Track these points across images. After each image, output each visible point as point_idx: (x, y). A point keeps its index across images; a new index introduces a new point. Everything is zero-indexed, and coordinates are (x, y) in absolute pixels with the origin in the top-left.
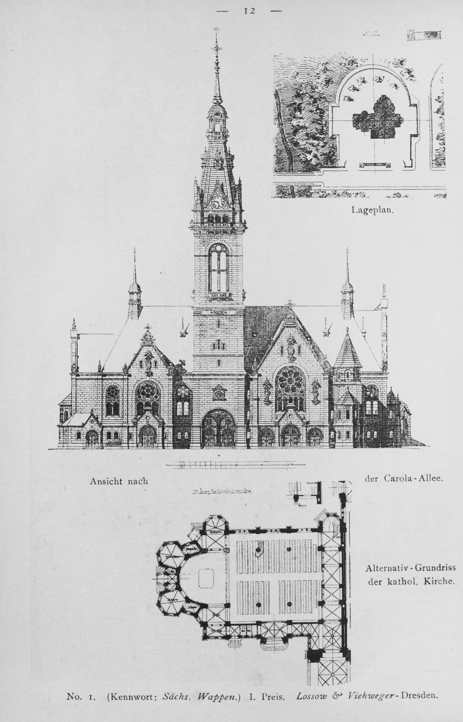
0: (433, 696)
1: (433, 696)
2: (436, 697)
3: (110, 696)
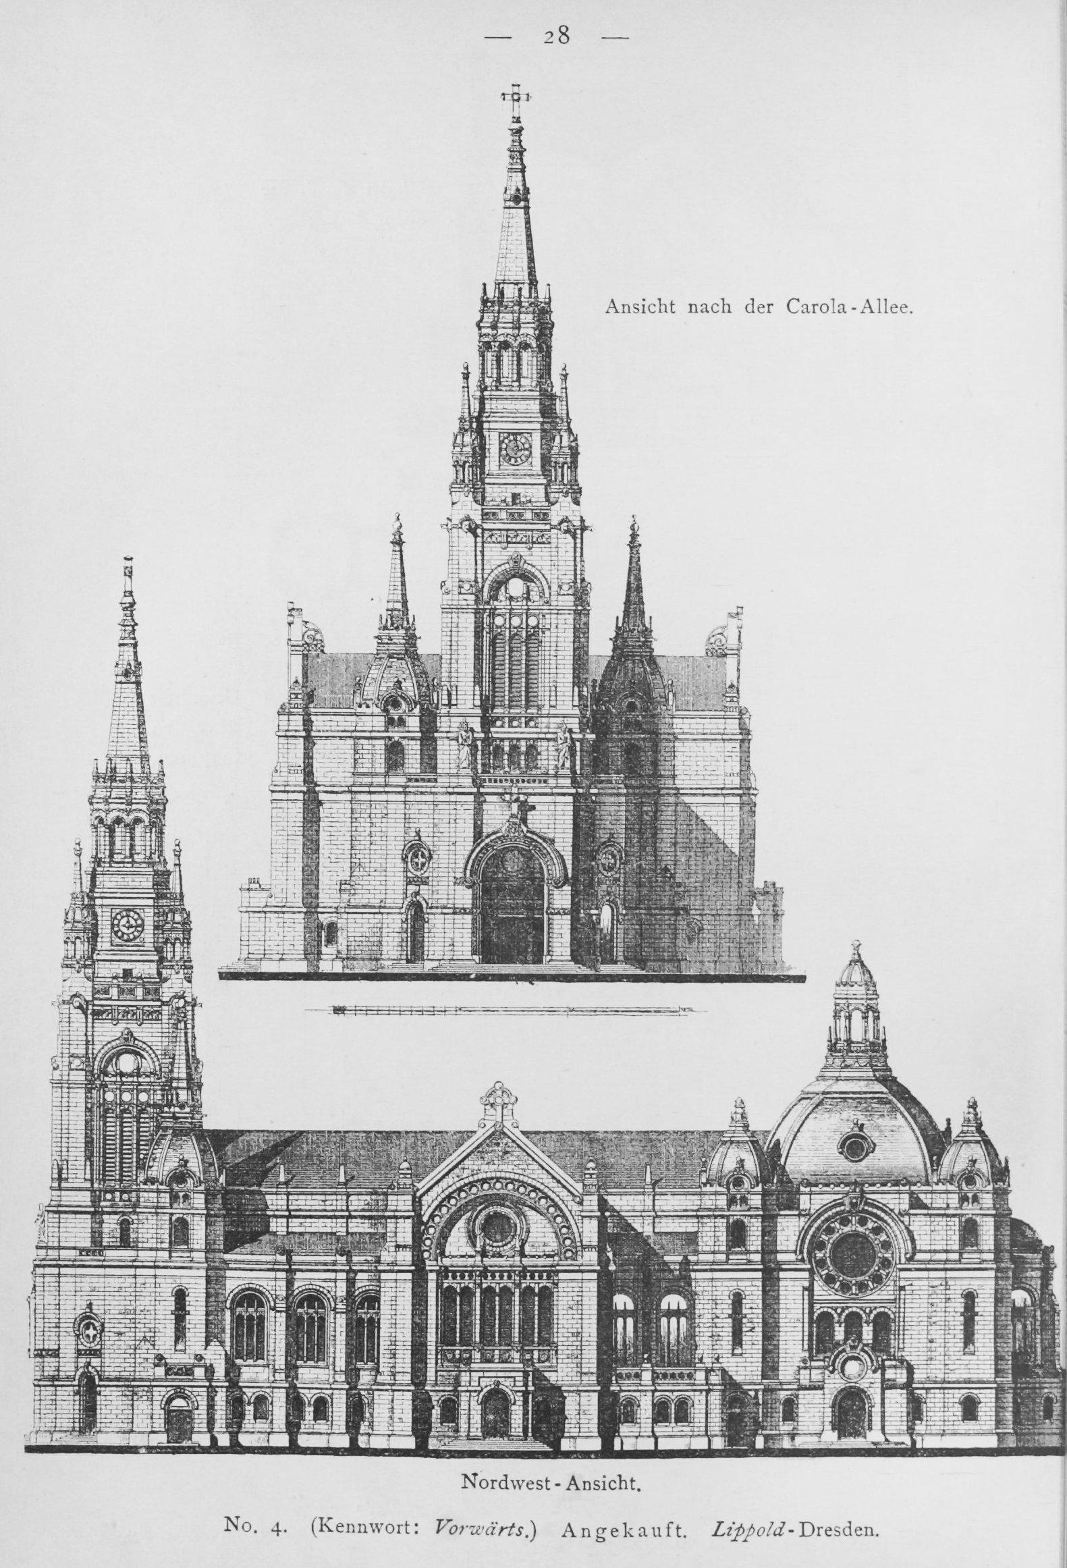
0: (869, 1532)
1: (869, 1532)
2: (875, 1533)
3: (318, 1523)
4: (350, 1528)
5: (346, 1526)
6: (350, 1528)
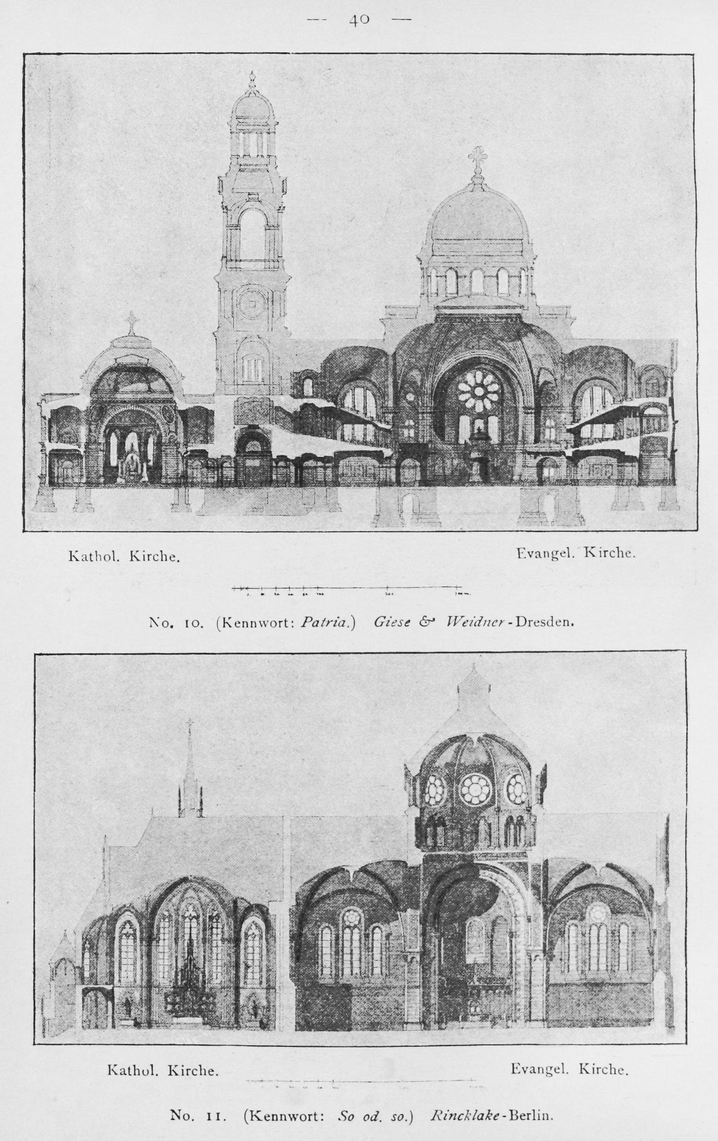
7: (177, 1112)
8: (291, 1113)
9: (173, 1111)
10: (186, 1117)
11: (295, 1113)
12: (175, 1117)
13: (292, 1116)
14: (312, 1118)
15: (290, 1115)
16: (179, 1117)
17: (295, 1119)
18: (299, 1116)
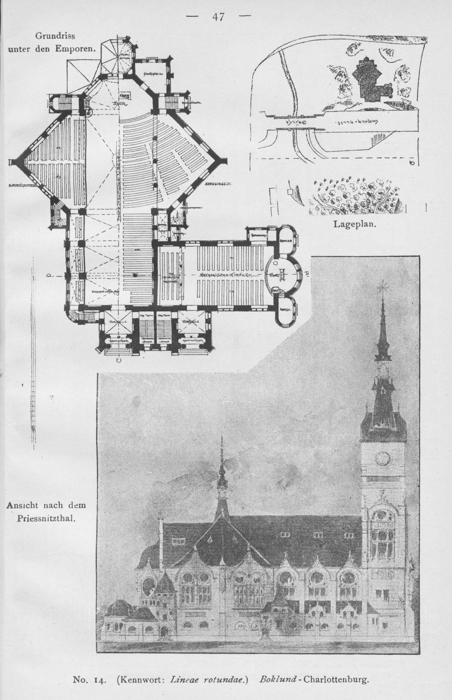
4: (134, 681)
5: (132, 680)
6: (134, 681)
7: (78, 678)
8: (145, 678)
9: (75, 677)
10: (83, 680)
11: (147, 678)
12: (76, 681)
13: (145, 680)
14: (157, 681)
15: (144, 679)
16: (78, 681)
17: (147, 682)
18: (149, 680)
